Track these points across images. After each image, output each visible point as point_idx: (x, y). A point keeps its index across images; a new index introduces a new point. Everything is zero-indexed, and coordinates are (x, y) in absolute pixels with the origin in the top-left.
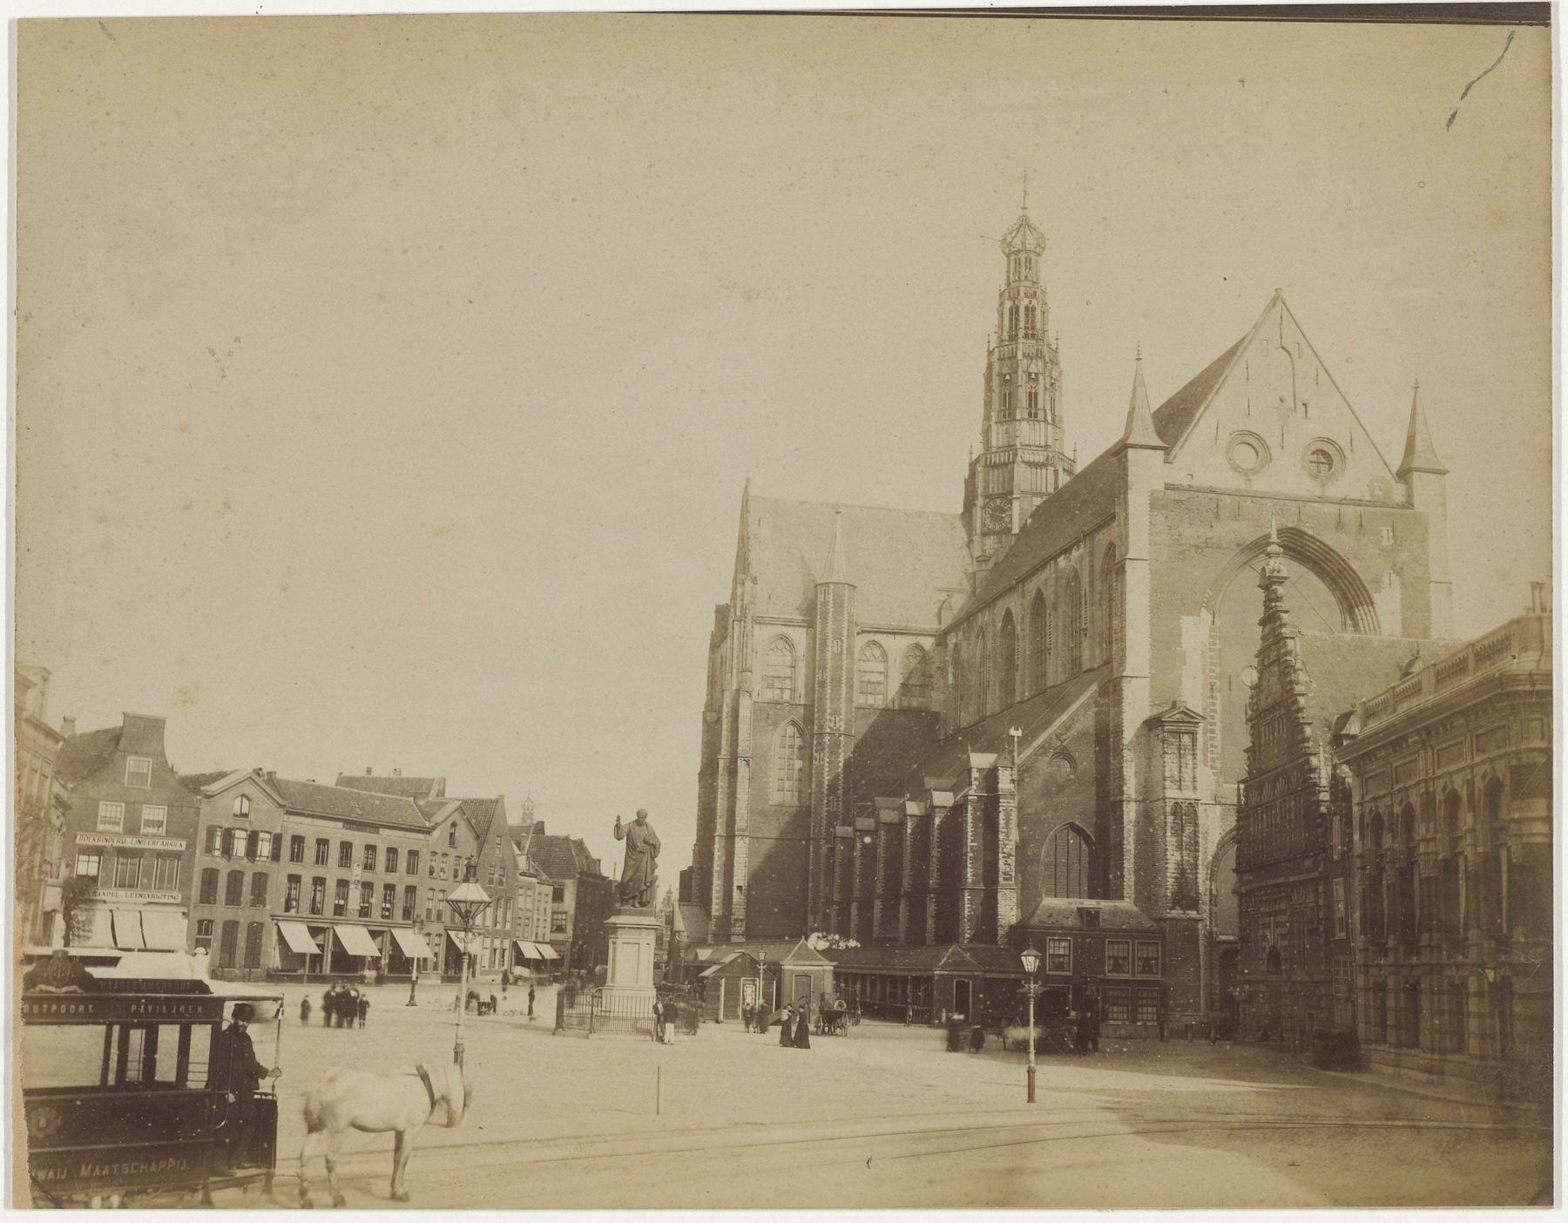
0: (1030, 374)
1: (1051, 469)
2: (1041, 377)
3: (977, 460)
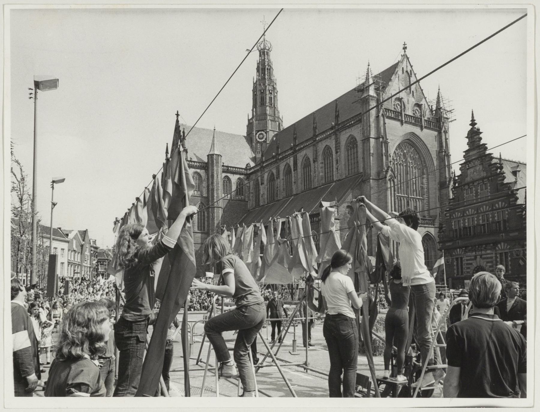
1: (277, 123)
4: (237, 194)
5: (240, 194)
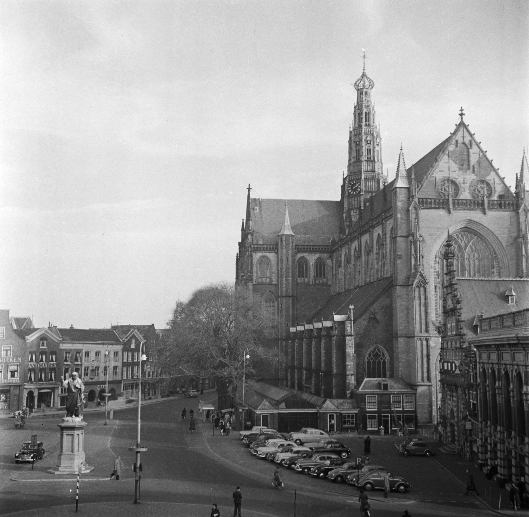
0: (367, 141)
2: (372, 142)
3: (346, 177)
4: (316, 276)
5: (321, 277)
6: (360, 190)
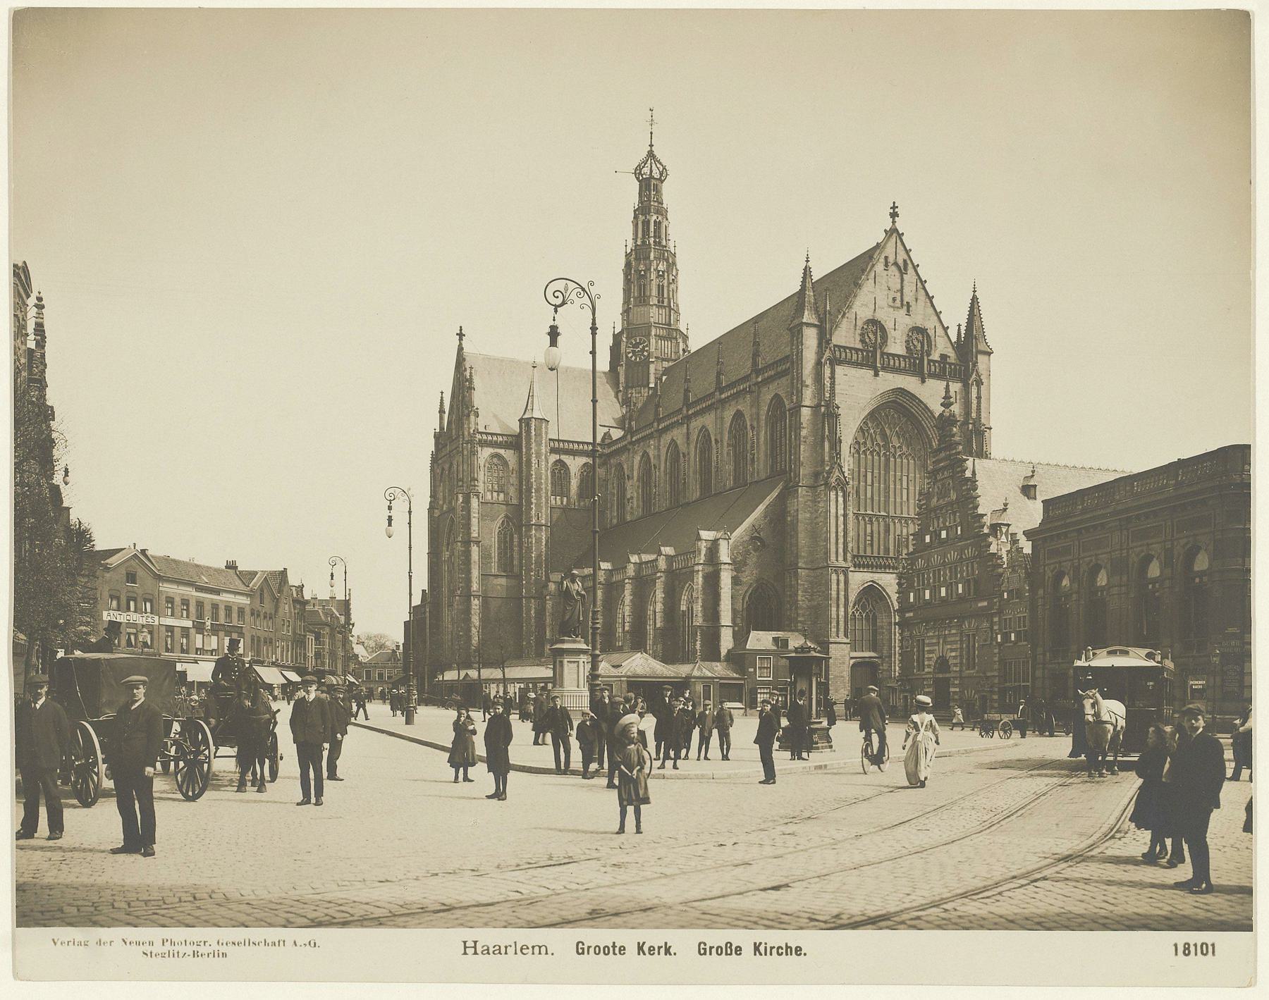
0: (659, 271)
2: (666, 274)
3: (621, 333)
4: (581, 495)
6: (649, 354)
